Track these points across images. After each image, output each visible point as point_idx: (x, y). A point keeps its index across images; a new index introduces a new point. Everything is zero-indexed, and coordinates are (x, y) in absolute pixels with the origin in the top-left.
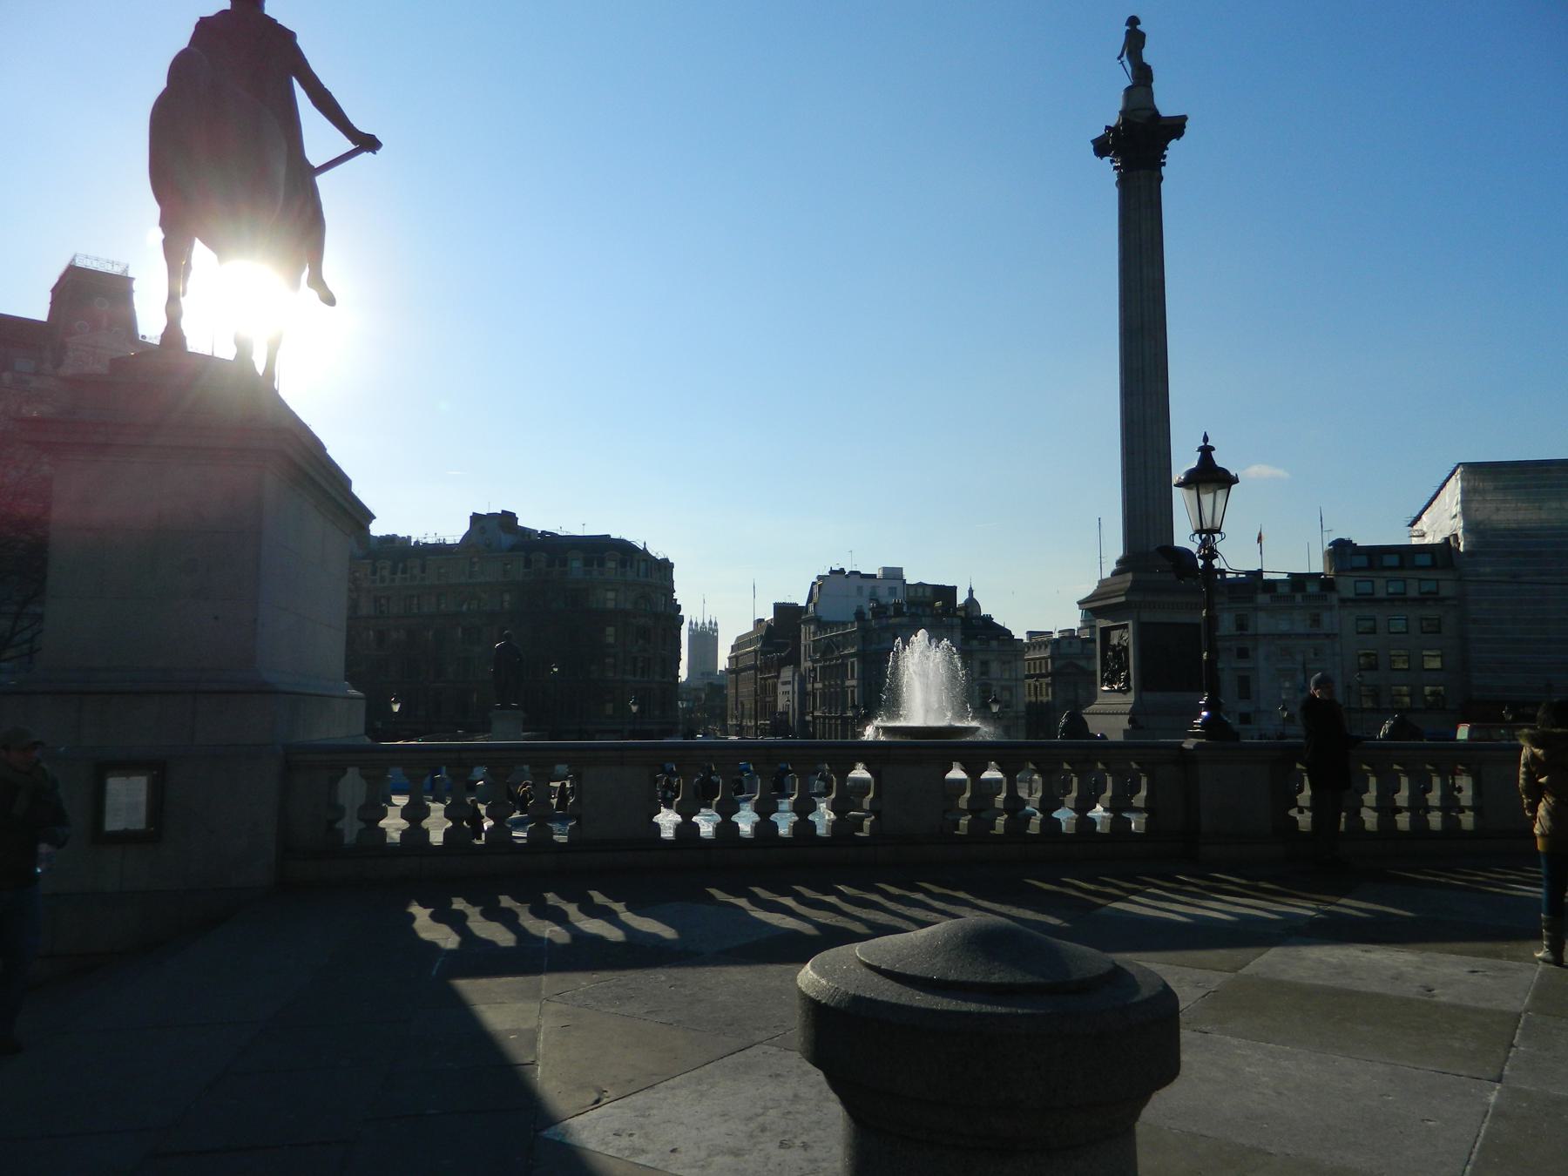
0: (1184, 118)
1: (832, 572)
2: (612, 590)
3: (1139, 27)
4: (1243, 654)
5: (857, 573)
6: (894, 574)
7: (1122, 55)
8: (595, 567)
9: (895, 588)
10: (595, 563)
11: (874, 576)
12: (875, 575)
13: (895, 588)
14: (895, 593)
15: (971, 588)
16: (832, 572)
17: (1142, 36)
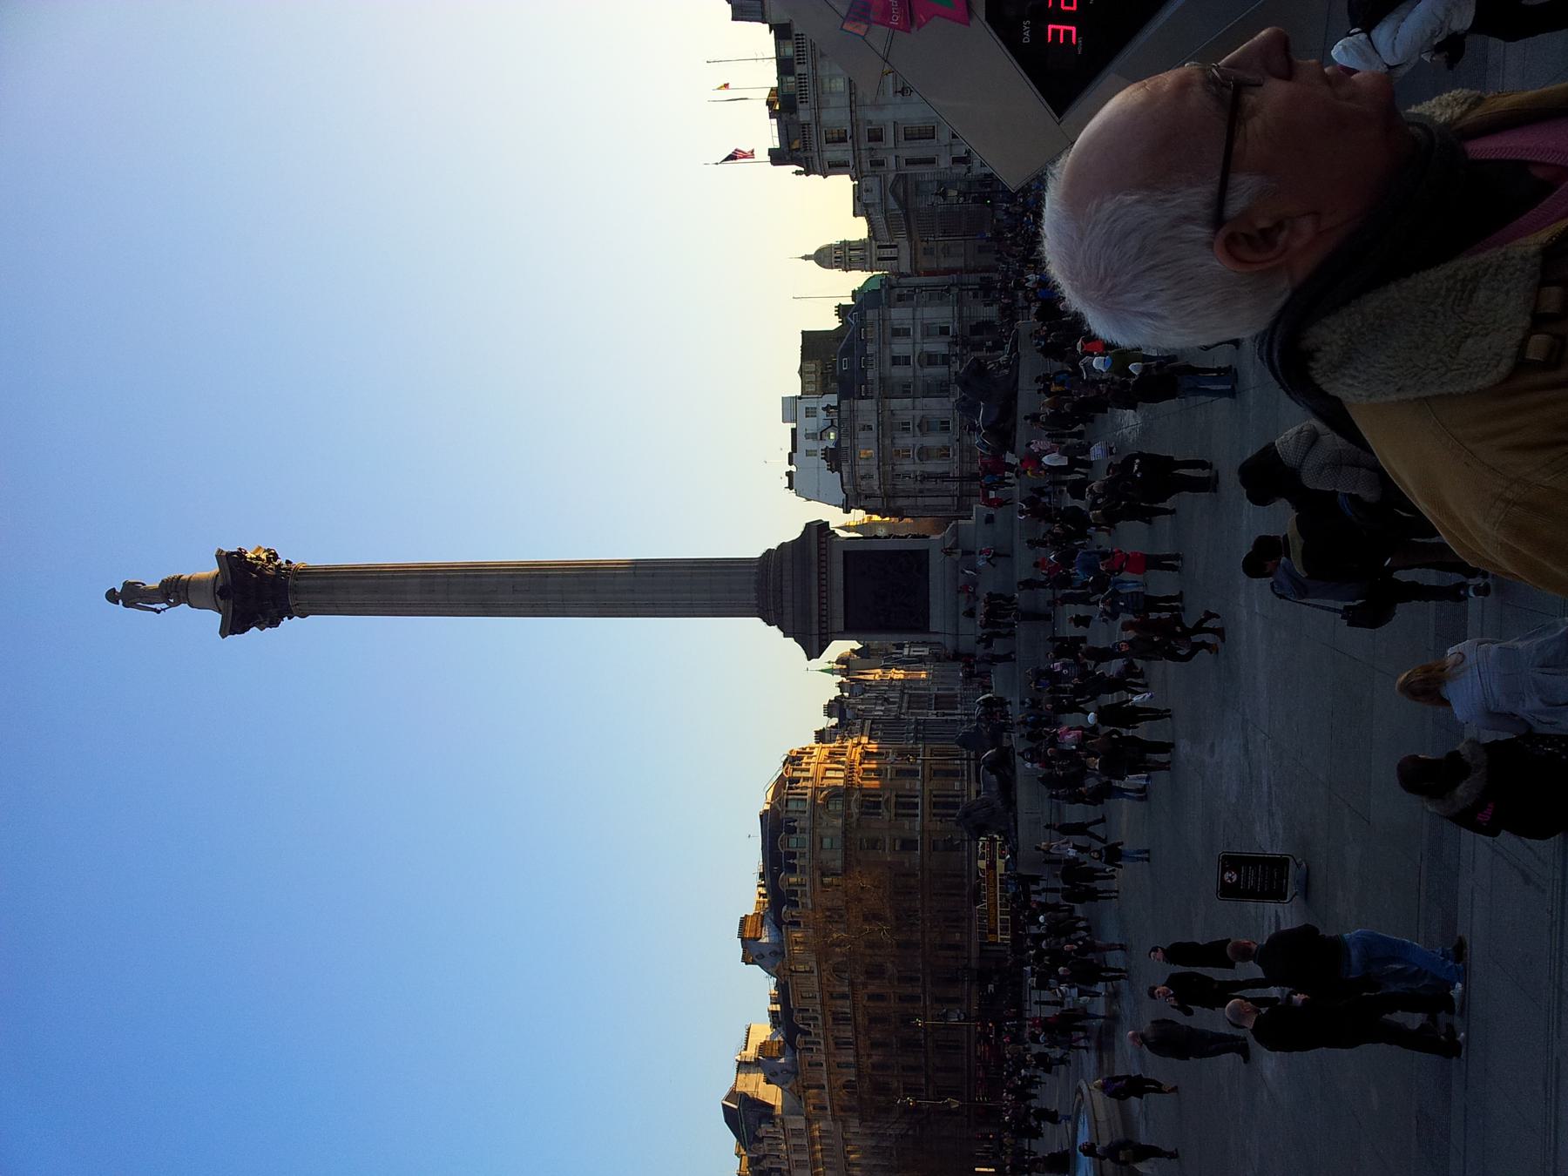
0: (220, 551)
1: (790, 487)
2: (822, 842)
3: (119, 590)
4: (876, 136)
5: (790, 456)
6: (791, 408)
7: (155, 610)
8: (795, 861)
9: (807, 408)
10: (791, 861)
11: (794, 431)
12: (792, 429)
13: (807, 408)
14: (812, 408)
15: (802, 258)
16: (790, 487)
17: (128, 586)
